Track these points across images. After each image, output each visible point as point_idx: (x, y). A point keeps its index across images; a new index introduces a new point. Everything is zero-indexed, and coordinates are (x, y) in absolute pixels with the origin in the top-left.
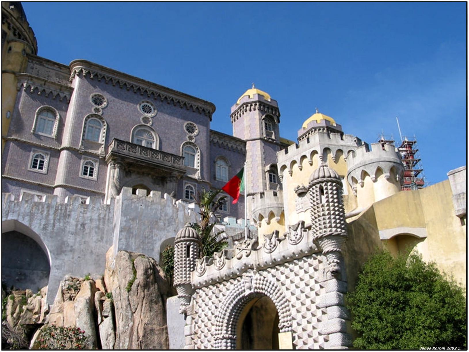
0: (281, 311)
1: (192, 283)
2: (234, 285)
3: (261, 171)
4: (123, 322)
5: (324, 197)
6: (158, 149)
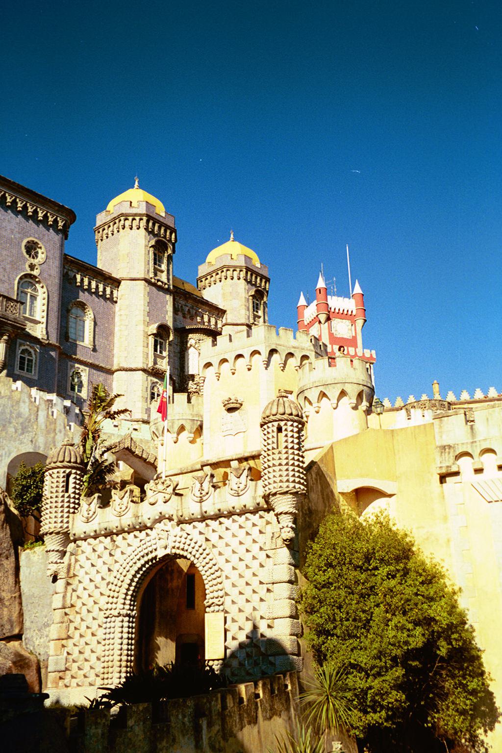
1: (72, 532)
2: (141, 541)
3: (142, 333)
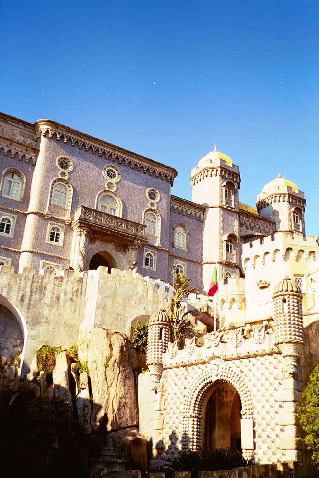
0: (244, 396)
2: (203, 370)
3: (219, 240)
4: (100, 395)
5: (286, 305)
6: (121, 217)
